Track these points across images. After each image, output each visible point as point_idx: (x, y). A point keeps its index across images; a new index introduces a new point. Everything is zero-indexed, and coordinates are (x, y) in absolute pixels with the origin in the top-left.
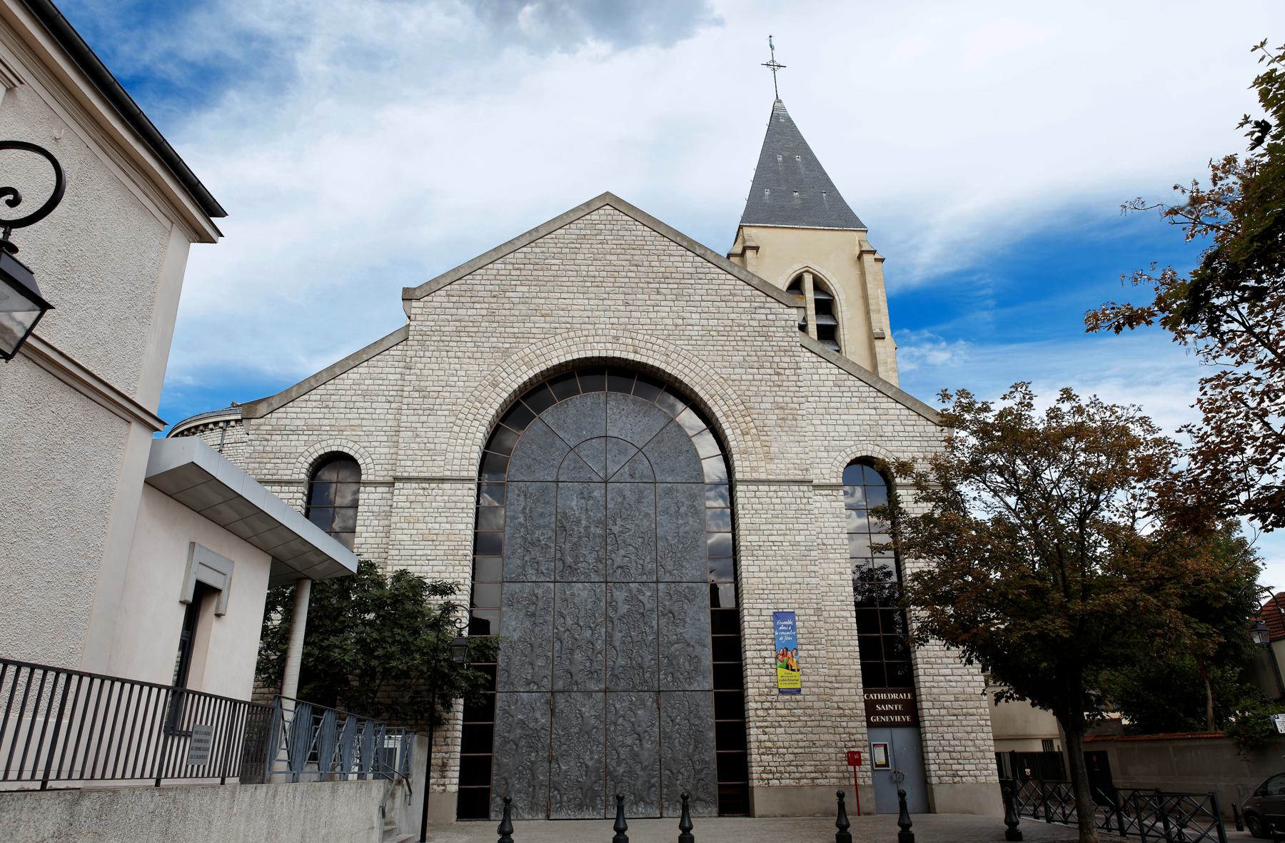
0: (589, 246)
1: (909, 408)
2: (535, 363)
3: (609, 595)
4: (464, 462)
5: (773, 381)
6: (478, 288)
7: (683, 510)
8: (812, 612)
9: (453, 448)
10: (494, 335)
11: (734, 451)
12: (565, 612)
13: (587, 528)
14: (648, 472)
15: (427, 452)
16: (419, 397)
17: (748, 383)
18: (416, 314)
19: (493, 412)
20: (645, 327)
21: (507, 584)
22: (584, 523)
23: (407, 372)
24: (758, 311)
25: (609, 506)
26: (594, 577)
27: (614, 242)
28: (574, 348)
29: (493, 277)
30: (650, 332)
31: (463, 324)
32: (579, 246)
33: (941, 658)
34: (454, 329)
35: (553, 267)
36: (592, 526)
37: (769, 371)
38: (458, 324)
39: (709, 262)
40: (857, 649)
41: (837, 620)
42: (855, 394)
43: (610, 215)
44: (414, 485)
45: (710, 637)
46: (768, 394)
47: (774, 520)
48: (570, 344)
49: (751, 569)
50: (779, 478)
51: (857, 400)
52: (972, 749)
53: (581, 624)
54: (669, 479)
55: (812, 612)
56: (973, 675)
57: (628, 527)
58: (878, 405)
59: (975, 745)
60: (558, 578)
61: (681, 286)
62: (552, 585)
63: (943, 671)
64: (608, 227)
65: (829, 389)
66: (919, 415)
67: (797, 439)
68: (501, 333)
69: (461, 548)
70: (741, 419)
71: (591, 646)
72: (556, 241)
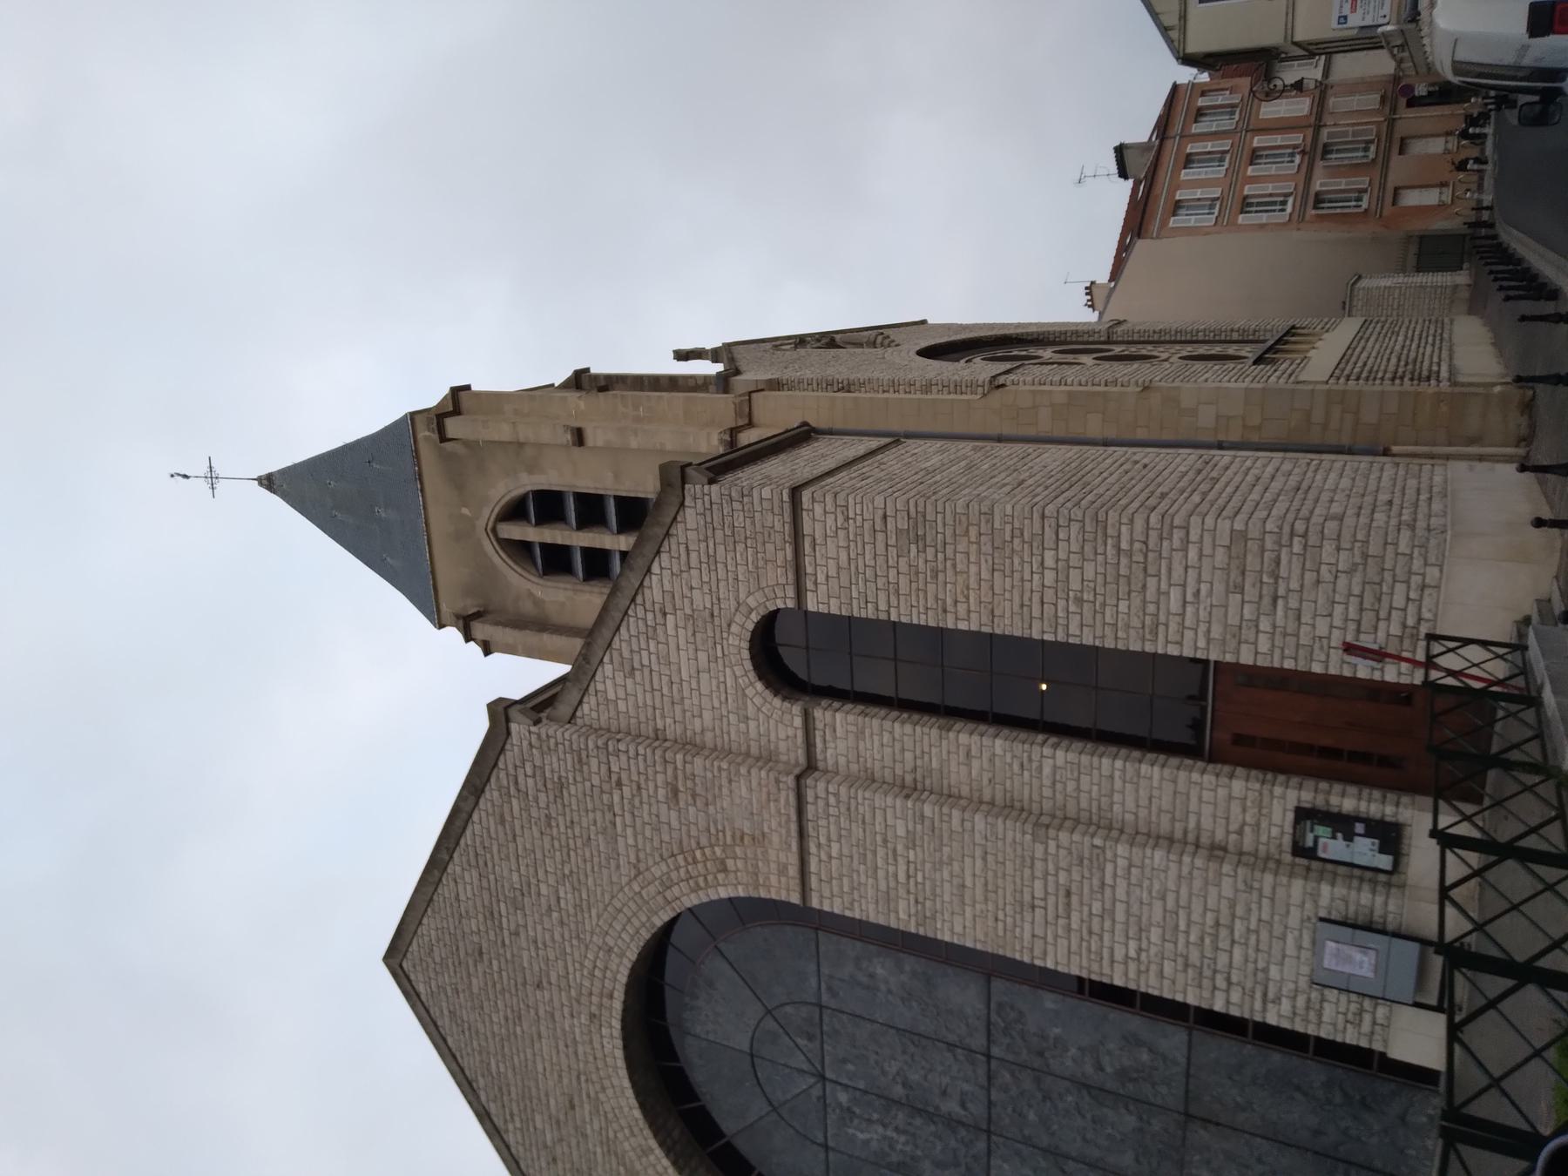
1: (658, 552)
20: (571, 969)
24: (522, 787)
26: (981, 1145)
33: (1144, 602)
41: (1059, 786)
49: (958, 929)
51: (652, 644)
52: (1357, 579)
54: (813, 982)
56: (1186, 541)
59: (1350, 572)
61: (501, 898)
63: (1175, 606)
67: (724, 782)
70: (700, 866)
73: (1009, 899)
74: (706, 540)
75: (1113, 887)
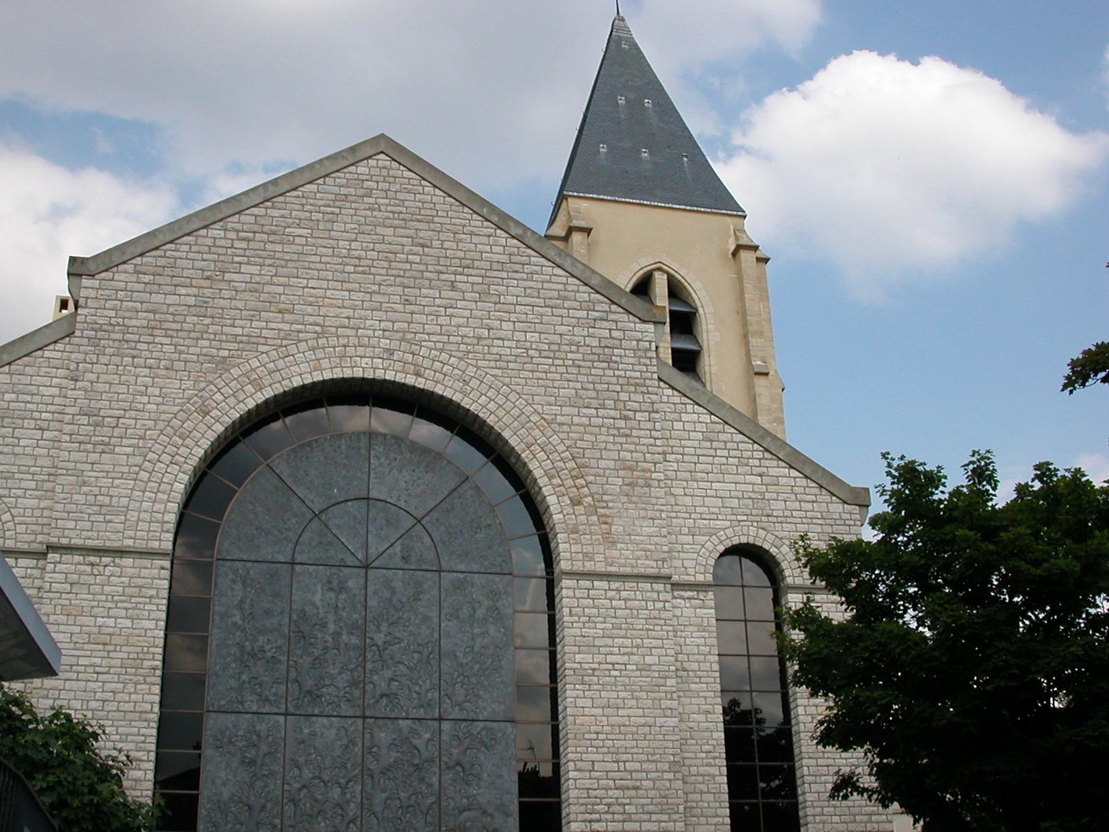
0: (352, 212)
1: (806, 477)
2: (266, 383)
3: (367, 736)
4: (154, 526)
5: (618, 429)
6: (184, 263)
7: (480, 613)
8: (666, 767)
9: (137, 505)
10: (205, 336)
11: (558, 528)
12: (301, 760)
13: (337, 634)
14: (431, 555)
15: (98, 508)
16: (88, 425)
17: (582, 429)
18: (87, 298)
19: (200, 452)
20: (434, 338)
21: (213, 715)
22: (332, 627)
23: (71, 384)
24: (598, 324)
25: (370, 603)
26: (345, 709)
27: (389, 209)
28: (325, 363)
29: (207, 249)
30: (440, 345)
31: (157, 317)
32: (337, 210)
34: (145, 323)
35: (298, 240)
36: (344, 632)
37: (613, 413)
38: (151, 316)
39: (529, 247)
40: (728, 820)
41: (700, 779)
42: (732, 453)
43: (385, 168)
44: (77, 558)
45: (516, 802)
46: (610, 446)
47: (615, 631)
48: (318, 357)
49: (580, 702)
50: (623, 570)
53: (326, 778)
54: (462, 567)
55: (666, 767)
57: (398, 635)
58: (765, 470)
60: (291, 709)
61: (487, 280)
62: (281, 719)
64: (381, 185)
65: (696, 444)
66: (821, 487)
67: (650, 514)
68: (215, 335)
69: (148, 656)
70: (569, 482)
71: (340, 811)
72: (304, 201)
73: (618, 744)
74: (822, 518)
75: (650, 821)
